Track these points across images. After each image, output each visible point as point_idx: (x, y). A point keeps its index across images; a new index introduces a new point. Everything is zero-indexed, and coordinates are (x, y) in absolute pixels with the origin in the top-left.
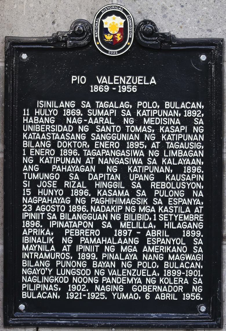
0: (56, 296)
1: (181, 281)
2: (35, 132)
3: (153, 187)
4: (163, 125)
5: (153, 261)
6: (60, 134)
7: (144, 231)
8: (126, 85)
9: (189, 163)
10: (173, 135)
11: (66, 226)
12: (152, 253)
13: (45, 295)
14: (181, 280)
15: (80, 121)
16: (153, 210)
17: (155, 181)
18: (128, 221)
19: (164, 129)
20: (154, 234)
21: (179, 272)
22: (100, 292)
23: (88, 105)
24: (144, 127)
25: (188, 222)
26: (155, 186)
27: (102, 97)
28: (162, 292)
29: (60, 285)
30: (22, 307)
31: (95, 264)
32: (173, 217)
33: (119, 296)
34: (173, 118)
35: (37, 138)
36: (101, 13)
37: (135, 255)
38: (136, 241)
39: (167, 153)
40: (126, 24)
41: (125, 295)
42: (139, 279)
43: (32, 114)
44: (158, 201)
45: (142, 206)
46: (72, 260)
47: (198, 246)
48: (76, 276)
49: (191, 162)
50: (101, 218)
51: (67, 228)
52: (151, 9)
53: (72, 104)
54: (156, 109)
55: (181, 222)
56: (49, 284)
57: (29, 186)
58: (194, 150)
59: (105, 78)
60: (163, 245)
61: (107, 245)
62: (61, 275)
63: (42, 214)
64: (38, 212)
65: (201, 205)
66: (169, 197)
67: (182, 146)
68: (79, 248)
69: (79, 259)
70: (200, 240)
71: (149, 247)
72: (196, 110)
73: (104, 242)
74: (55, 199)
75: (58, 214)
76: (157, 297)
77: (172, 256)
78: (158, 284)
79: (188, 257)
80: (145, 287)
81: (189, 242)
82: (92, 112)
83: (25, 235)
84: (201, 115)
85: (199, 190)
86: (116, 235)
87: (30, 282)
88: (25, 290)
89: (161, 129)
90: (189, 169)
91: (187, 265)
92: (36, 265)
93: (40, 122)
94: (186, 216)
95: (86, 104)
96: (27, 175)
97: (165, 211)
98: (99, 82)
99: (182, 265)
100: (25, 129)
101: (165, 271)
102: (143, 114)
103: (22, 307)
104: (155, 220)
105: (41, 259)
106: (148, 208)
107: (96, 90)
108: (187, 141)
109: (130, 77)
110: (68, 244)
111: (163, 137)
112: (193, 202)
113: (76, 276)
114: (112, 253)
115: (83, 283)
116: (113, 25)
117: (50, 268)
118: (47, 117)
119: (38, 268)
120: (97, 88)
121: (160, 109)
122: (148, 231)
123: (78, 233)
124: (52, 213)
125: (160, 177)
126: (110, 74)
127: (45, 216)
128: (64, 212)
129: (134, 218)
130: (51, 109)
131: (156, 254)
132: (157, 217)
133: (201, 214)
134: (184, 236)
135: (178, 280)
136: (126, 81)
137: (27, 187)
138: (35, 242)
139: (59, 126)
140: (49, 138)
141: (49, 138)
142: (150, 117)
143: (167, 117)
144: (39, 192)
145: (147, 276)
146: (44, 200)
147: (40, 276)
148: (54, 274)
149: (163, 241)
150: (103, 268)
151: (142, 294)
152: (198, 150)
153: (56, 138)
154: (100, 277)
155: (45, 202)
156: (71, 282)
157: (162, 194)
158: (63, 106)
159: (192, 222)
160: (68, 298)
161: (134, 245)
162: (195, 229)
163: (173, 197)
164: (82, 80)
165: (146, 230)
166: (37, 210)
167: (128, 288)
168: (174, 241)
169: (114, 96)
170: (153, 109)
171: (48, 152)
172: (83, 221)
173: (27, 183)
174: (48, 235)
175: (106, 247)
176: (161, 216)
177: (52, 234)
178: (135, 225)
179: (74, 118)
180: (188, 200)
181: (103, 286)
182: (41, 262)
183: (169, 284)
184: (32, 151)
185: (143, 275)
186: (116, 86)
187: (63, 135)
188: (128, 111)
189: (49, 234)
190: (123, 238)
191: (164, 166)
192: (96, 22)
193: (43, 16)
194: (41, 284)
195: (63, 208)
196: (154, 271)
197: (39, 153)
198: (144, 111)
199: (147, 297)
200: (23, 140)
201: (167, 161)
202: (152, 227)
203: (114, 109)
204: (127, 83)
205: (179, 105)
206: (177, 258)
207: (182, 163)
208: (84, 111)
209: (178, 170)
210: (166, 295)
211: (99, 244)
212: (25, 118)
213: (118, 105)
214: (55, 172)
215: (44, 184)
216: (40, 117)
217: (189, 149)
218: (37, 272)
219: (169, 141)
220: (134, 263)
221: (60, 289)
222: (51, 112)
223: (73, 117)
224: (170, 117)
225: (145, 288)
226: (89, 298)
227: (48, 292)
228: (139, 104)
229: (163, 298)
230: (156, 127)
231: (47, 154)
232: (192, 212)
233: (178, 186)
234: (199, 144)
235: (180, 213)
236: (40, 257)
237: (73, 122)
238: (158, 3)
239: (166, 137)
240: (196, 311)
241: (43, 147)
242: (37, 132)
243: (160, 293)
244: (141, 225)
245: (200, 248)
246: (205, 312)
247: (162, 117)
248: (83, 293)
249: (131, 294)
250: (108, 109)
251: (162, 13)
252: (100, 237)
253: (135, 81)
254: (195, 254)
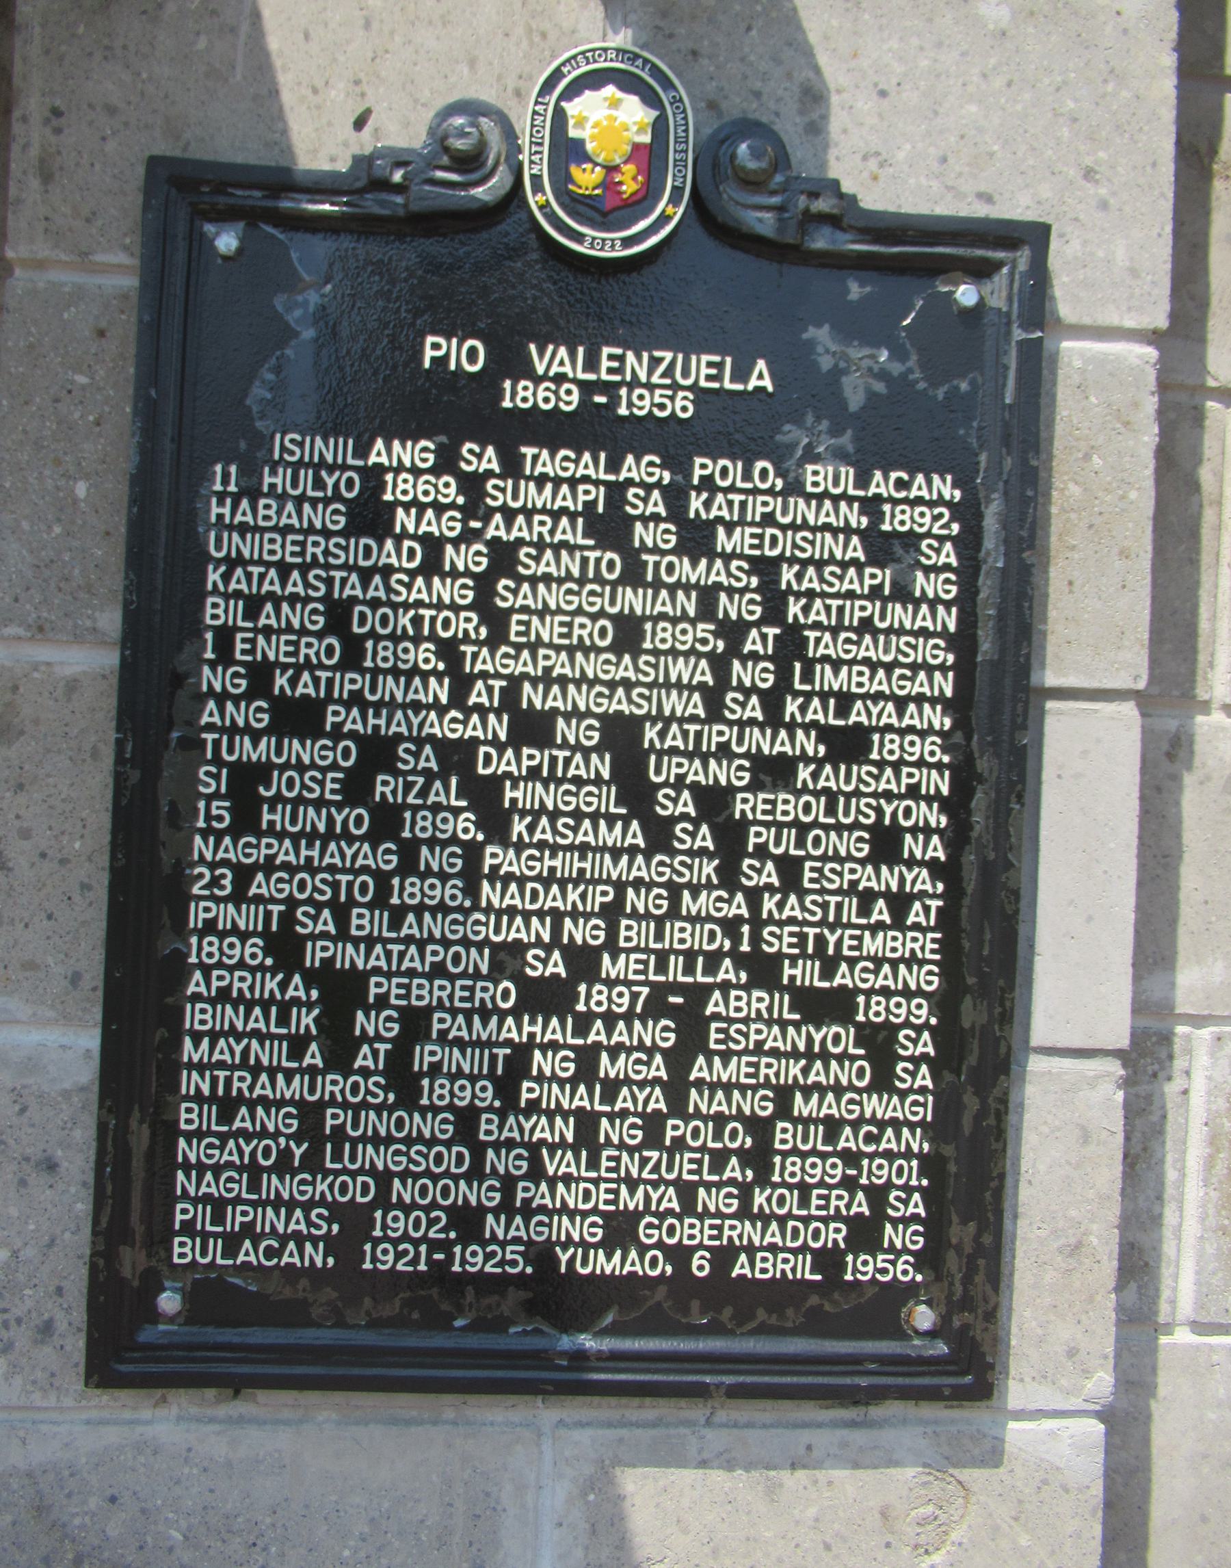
0: (317, 1256)
1: (842, 1204)
2: (261, 562)
3: (743, 812)
4: (792, 560)
5: (732, 1118)
6: (366, 576)
7: (699, 994)
8: (651, 387)
9: (894, 721)
10: (835, 603)
11: (372, 962)
12: (728, 1087)
13: (269, 1253)
14: (839, 1197)
15: (450, 526)
16: (739, 907)
17: (755, 786)
18: (637, 949)
19: (799, 577)
20: (738, 1009)
21: (834, 1166)
22: (503, 1244)
23: (490, 460)
24: (719, 563)
25: (878, 961)
26: (753, 809)
27: (551, 429)
28: (762, 1248)
29: (336, 1211)
30: (169, 1302)
31: (487, 1128)
32: (820, 941)
33: (585, 1263)
34: (835, 531)
35: (266, 587)
36: (557, 75)
37: (658, 1091)
38: (661, 1033)
39: (807, 677)
40: (659, 128)
41: (609, 1257)
42: (671, 1190)
43: (252, 493)
44: (759, 871)
45: (695, 890)
46: (391, 1109)
47: (916, 1061)
48: (404, 1175)
49: (901, 715)
50: (523, 936)
51: (377, 971)
52: (758, 95)
53: (418, 452)
54: (771, 492)
55: (852, 962)
56: (291, 1205)
57: (223, 790)
58: (914, 667)
59: (563, 352)
60: (774, 1052)
61: (544, 1048)
62: (345, 1171)
63: (276, 909)
64: (258, 899)
65: (934, 896)
66: (809, 857)
67: (868, 649)
68: (425, 1055)
69: (425, 1101)
70: (926, 1035)
71: (717, 1060)
72: (931, 504)
73: (532, 1036)
74: (333, 846)
75: (341, 913)
76: (741, 1268)
77: (807, 1100)
78: (745, 1212)
79: (874, 1105)
80: (692, 1226)
81: (879, 1044)
82: (503, 490)
83: (197, 997)
84: (946, 526)
85: (928, 831)
86: (581, 1007)
87: (207, 1199)
88: (188, 1228)
89: (787, 575)
90: (892, 743)
91: (869, 1139)
92: (237, 1124)
93: (284, 521)
94: (873, 936)
95: (480, 457)
96: (217, 744)
97: (787, 913)
98: (540, 370)
99: (847, 1139)
100: (219, 548)
101: (777, 1159)
102: (714, 513)
103: (169, 1302)
104: (745, 948)
105: (263, 1100)
106: (719, 899)
107: (525, 400)
108: (889, 631)
109: (668, 356)
110: (378, 1038)
111: (794, 609)
112: (902, 880)
113: (404, 1175)
114: (562, 1083)
115: (434, 1205)
116: (608, 131)
117: (298, 1137)
118: (314, 502)
119: (248, 1136)
120: (529, 394)
121: (785, 493)
122: (717, 995)
123: (424, 994)
124: (319, 906)
125: (773, 772)
126: (586, 334)
127: (288, 919)
128: (370, 906)
129: (659, 937)
130: (331, 469)
131: (743, 1088)
132: (756, 939)
133: (933, 930)
134: (860, 1018)
135: (827, 1198)
136: (650, 373)
137: (216, 795)
138: (240, 1026)
139: (363, 541)
140: (316, 589)
141: (316, 589)
142: (742, 522)
143: (814, 530)
144: (266, 817)
145: (702, 1183)
146: (285, 853)
147: (254, 1172)
148: (313, 1163)
149: (773, 1038)
150: (523, 1145)
151: (680, 1255)
152: (930, 670)
153: (348, 592)
154: (508, 1184)
155: (292, 858)
156: (383, 1200)
157: (777, 843)
158: (384, 460)
159: (894, 964)
160: (368, 1266)
161: (651, 1051)
162: (907, 993)
163: (824, 858)
164: (464, 354)
165: (707, 990)
166: (253, 891)
167: (620, 1230)
168: (818, 1038)
169: (594, 427)
170: (755, 492)
171: (310, 649)
172: (446, 943)
173: (217, 777)
174: (296, 1001)
175: (537, 1054)
176: (772, 934)
177: (315, 994)
178: (662, 967)
179: (430, 513)
180: (884, 869)
181: (518, 1220)
182: (260, 1111)
183: (790, 1216)
184: (244, 641)
185: (686, 1177)
186: (609, 389)
187: (377, 579)
188: (656, 494)
189: (301, 994)
190: (610, 1019)
191: (791, 727)
192: (535, 113)
193: (315, 91)
194: (254, 1204)
195: (364, 888)
196: (734, 1160)
197: (271, 650)
198: (720, 498)
199: (700, 1266)
200: (204, 595)
201: (803, 709)
202: (731, 976)
203: (597, 483)
204: (655, 379)
205: (863, 481)
206: (830, 1107)
207: (863, 719)
208: (473, 485)
209: (848, 745)
210: (774, 1258)
211: (508, 1043)
212: (221, 503)
213: (614, 465)
214: (337, 733)
215: (291, 781)
216: (282, 498)
217: (895, 664)
218: (241, 1153)
219: (817, 626)
220: (653, 1125)
221: (335, 1228)
222: (330, 482)
223: (422, 508)
224: (827, 527)
225: (692, 1232)
226: (456, 1268)
227: (284, 1239)
228: (701, 467)
229: (764, 1271)
230: (766, 568)
231: (307, 656)
232: (899, 922)
233: (846, 814)
234: (936, 647)
235: (850, 925)
236: (258, 1091)
237: (423, 528)
238: (789, 76)
239: (806, 610)
240: (898, 1331)
241: (289, 629)
242: (268, 565)
243: (751, 1250)
244: (689, 969)
245: (924, 1069)
246: (931, 1334)
247: (793, 527)
248: (434, 1245)
249: (633, 1254)
250: (573, 482)
251: (802, 112)
252: (516, 1012)
253: (685, 374)
254: (903, 1094)
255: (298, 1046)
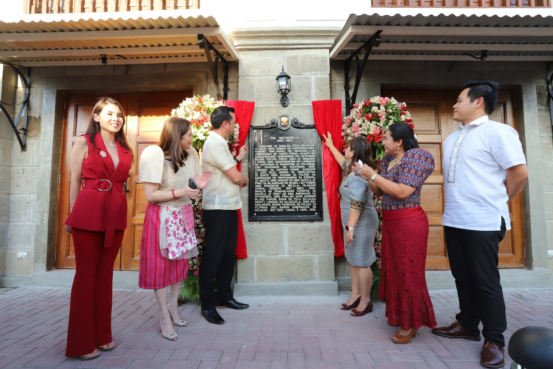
0: (266, 210)
15: (274, 151)
31: (279, 199)
38: (293, 191)
53: (271, 146)
68: (274, 194)
123: (274, 189)
125: (301, 169)
148: (266, 203)
151: (296, 209)
164: (274, 138)
167: (291, 207)
169: (285, 143)
171: (263, 162)
199: (297, 210)
209: (307, 167)
220: (293, 198)
225: (297, 207)
255: (264, 193)
